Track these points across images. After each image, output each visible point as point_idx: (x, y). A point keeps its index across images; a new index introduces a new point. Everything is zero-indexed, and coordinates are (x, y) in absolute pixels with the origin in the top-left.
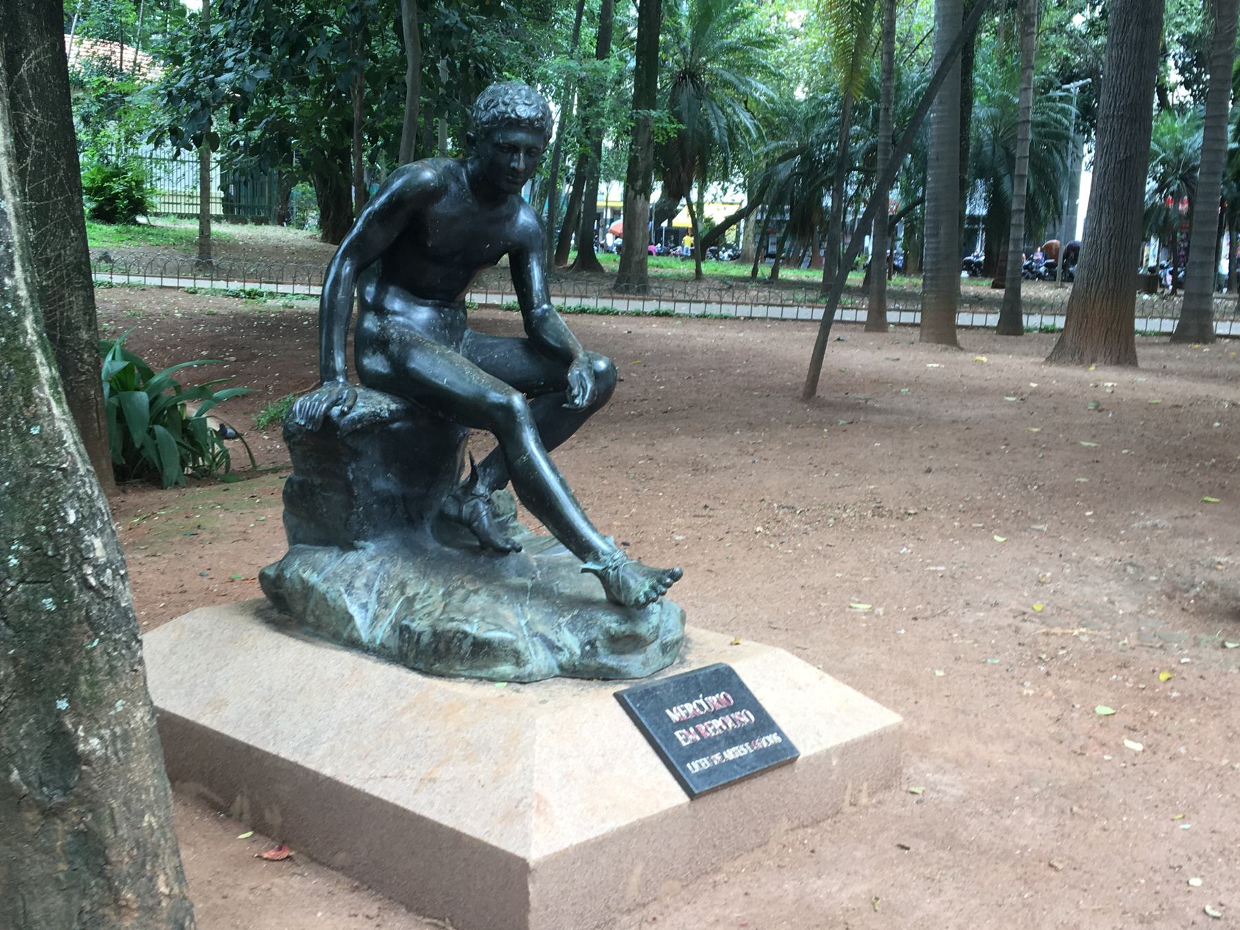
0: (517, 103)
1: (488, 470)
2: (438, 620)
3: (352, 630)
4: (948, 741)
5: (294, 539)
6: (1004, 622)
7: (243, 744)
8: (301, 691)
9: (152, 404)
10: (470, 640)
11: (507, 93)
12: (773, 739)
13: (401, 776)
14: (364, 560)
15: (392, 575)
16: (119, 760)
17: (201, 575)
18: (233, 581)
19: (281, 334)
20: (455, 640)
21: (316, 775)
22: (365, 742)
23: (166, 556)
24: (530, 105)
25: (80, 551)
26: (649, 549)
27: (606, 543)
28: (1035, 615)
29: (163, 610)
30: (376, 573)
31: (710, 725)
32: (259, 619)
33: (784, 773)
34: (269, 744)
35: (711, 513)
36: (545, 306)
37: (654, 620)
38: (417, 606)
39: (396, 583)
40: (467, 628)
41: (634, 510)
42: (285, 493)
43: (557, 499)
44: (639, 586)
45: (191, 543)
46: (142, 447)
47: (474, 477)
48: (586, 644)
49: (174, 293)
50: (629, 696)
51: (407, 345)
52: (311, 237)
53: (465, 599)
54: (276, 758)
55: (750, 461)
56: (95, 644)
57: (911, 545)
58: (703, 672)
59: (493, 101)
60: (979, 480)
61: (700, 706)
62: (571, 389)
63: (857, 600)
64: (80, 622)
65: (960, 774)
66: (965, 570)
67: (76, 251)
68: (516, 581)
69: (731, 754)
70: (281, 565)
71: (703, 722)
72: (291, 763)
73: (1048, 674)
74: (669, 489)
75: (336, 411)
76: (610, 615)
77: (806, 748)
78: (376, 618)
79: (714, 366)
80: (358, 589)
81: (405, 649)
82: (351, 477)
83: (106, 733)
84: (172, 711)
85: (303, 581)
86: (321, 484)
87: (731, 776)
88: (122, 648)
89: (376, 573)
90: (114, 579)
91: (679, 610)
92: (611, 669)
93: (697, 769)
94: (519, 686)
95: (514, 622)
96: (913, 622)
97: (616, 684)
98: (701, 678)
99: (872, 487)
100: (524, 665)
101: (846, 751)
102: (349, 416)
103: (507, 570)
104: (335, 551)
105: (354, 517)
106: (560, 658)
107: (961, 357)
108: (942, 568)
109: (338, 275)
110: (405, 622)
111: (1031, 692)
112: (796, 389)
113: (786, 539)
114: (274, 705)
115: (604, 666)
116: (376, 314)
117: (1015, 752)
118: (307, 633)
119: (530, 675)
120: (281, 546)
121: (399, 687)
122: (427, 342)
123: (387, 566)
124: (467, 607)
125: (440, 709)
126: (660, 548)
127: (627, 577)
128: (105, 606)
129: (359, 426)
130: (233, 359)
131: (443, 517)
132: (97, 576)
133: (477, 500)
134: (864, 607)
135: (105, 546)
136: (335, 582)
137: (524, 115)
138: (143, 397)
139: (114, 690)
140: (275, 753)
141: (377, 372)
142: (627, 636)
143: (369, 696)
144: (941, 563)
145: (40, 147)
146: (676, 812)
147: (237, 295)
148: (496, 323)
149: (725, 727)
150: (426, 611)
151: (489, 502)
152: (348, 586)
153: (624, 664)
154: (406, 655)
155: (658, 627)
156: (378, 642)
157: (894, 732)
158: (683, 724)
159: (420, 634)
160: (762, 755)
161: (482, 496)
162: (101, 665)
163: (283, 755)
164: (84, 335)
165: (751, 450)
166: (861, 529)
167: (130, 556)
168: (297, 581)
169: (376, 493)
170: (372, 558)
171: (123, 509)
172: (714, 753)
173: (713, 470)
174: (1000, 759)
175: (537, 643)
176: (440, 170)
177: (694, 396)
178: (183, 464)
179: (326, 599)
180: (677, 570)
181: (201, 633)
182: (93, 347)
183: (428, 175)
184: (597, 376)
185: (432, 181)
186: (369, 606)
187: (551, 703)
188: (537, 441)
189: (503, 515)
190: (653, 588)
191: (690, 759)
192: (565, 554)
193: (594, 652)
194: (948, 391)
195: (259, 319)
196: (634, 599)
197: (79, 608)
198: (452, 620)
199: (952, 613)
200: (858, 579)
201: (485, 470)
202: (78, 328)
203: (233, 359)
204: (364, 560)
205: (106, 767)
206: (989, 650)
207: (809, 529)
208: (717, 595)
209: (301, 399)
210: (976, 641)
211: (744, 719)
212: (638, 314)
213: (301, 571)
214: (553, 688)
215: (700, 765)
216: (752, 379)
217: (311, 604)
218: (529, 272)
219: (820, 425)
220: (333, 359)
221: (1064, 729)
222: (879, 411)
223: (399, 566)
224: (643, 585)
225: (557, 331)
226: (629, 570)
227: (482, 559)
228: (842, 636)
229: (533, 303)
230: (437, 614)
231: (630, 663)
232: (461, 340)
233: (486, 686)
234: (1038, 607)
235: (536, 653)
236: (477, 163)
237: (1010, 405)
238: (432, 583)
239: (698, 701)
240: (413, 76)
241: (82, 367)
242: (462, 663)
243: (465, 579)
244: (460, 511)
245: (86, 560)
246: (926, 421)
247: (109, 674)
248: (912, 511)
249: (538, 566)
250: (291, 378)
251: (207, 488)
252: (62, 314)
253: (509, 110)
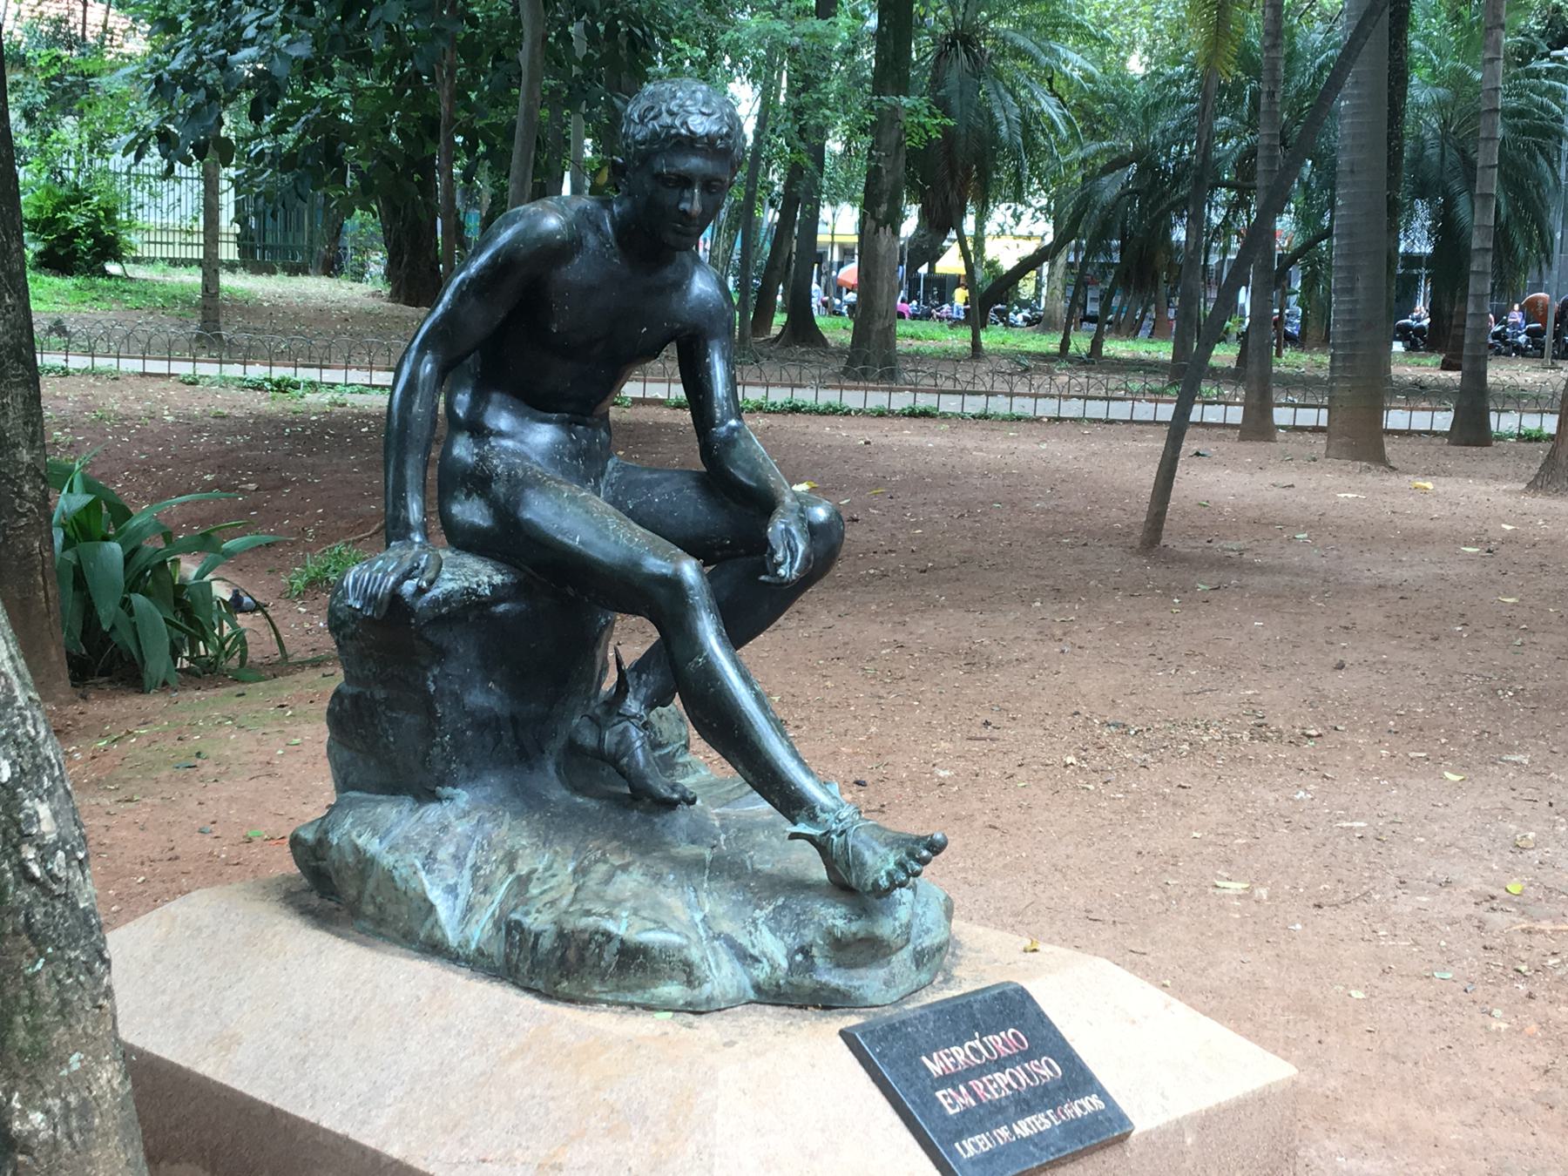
0: (691, 113)
1: (644, 677)
2: (566, 912)
3: (433, 927)
4: (1371, 1106)
5: (344, 784)
6: (1461, 912)
7: (264, 1105)
8: (354, 1023)
9: (128, 559)
10: (615, 945)
11: (674, 97)
12: (1092, 1103)
13: (509, 1159)
14: (452, 818)
15: (495, 840)
16: (74, 1146)
17: (201, 831)
18: (250, 841)
19: (328, 448)
20: (593, 946)
21: (376, 1156)
22: (453, 1105)
23: (144, 800)
24: (709, 115)
25: (17, 823)
26: (898, 790)
27: (828, 793)
28: (1508, 901)
29: (141, 888)
30: (471, 838)
31: (991, 1082)
32: (291, 909)
33: (1110, 1157)
34: (304, 1106)
35: (996, 734)
36: (733, 423)
37: (903, 914)
38: (534, 890)
39: (501, 853)
40: (610, 926)
41: (873, 729)
42: (330, 712)
43: (752, 726)
44: (880, 862)
45: (185, 781)
46: (113, 628)
47: (622, 688)
48: (797, 952)
49: (162, 384)
50: (864, 1036)
51: (519, 484)
52: (373, 295)
53: (608, 879)
54: (315, 1128)
55: (1057, 650)
56: (39, 966)
57: (1312, 787)
58: (980, 997)
59: (652, 108)
60: (1422, 681)
61: (975, 1051)
62: (773, 553)
63: (1226, 875)
64: (16, 933)
65: (1390, 1158)
66: (1398, 828)
67: (13, 326)
68: (686, 850)
69: (1024, 1128)
70: (324, 826)
71: (979, 1078)
72: (337, 1136)
73: (1530, 996)
74: (928, 695)
75: (409, 587)
76: (834, 906)
77: (1144, 1116)
78: (470, 908)
79: (1000, 497)
80: (443, 862)
81: (514, 958)
82: (432, 688)
83: (55, 1104)
84: (156, 1052)
85: (357, 850)
86: (386, 699)
87: (1025, 1163)
88: (80, 973)
89: (471, 838)
90: (68, 865)
91: (942, 898)
92: (837, 991)
93: (972, 1152)
94: (691, 1017)
95: (683, 914)
96: (1315, 911)
97: (843, 1015)
98: (976, 1006)
99: (1250, 692)
100: (700, 985)
101: (1206, 1122)
102: (429, 595)
103: (673, 834)
104: (408, 802)
105: (437, 750)
106: (755, 973)
107: (1392, 481)
108: (1363, 824)
109: (413, 375)
110: (515, 916)
111: (1504, 1026)
112: (1129, 534)
113: (1113, 777)
114: (312, 1044)
115: (824, 986)
116: (472, 436)
117: (1478, 1124)
118: (363, 931)
119: (709, 1000)
120: (324, 790)
121: (506, 1018)
122: (549, 479)
123: (488, 826)
124: (611, 892)
125: (569, 1055)
126: (915, 791)
127: (861, 847)
128: (54, 907)
129: (444, 610)
130: (252, 486)
131: (573, 749)
132: (43, 862)
133: (627, 723)
134: (1237, 887)
135: (55, 815)
136: (407, 851)
137: (700, 130)
138: (115, 549)
139: (67, 1037)
140: (313, 1120)
141: (472, 525)
142: (861, 940)
143: (459, 1033)
144: (1360, 816)
147: (258, 387)
148: (658, 427)
149: (1015, 1085)
150: (547, 898)
151: (646, 726)
152: (427, 858)
153: (856, 983)
154: (517, 966)
155: (909, 926)
156: (473, 946)
157: (1283, 1092)
158: (948, 1080)
159: (538, 935)
160: (1075, 1129)
161: (634, 716)
162: (48, 1000)
163: (325, 1124)
164: (25, 456)
165: (1058, 632)
166: (1233, 760)
167: (93, 802)
168: (348, 849)
169: (471, 714)
170: (466, 814)
171: (82, 725)
172: (998, 1126)
173: (999, 665)
174: (1453, 1136)
175: (720, 950)
176: (571, 214)
177: (968, 544)
178: (175, 653)
179: (393, 879)
180: (938, 836)
181: (199, 930)
182: (38, 474)
183: (552, 222)
184: (813, 530)
185: (558, 232)
186: (459, 890)
187: (741, 1043)
188: (719, 634)
189: (668, 744)
190: (901, 865)
191: (959, 1135)
192: (762, 808)
193: (809, 966)
194: (1369, 537)
195: (292, 423)
196: (870, 881)
197: (15, 912)
198: (588, 913)
199: (1377, 897)
200: (1227, 841)
201: (639, 677)
202: (16, 445)
203: (252, 486)
204: (452, 818)
205: (54, 1156)
206: (1437, 956)
207: (1150, 760)
208: (1005, 866)
209: (357, 568)
210: (1416, 943)
211: (1046, 1072)
212: (881, 414)
213: (354, 834)
214: (745, 1021)
215: (976, 1146)
216: (1059, 518)
217: (371, 884)
218: (708, 369)
219: (1168, 592)
220: (406, 507)
221: (1555, 1086)
222: (1262, 569)
223: (505, 827)
224: (885, 860)
225: (751, 460)
226: (863, 835)
227: (635, 815)
228: (1202, 934)
229: (712, 418)
230: (565, 902)
231: (866, 982)
232: (603, 474)
233: (640, 1018)
234: (1515, 888)
235: (718, 966)
236: (627, 203)
237: (1470, 559)
238: (556, 853)
239: (972, 1044)
240: (532, 55)
241: (20, 506)
242: (602, 980)
243: (608, 847)
244: (601, 740)
245: (25, 837)
246: (1338, 588)
247: (60, 1012)
248: (1313, 733)
249: (722, 826)
250: (342, 517)
251: (211, 692)
253: (677, 123)
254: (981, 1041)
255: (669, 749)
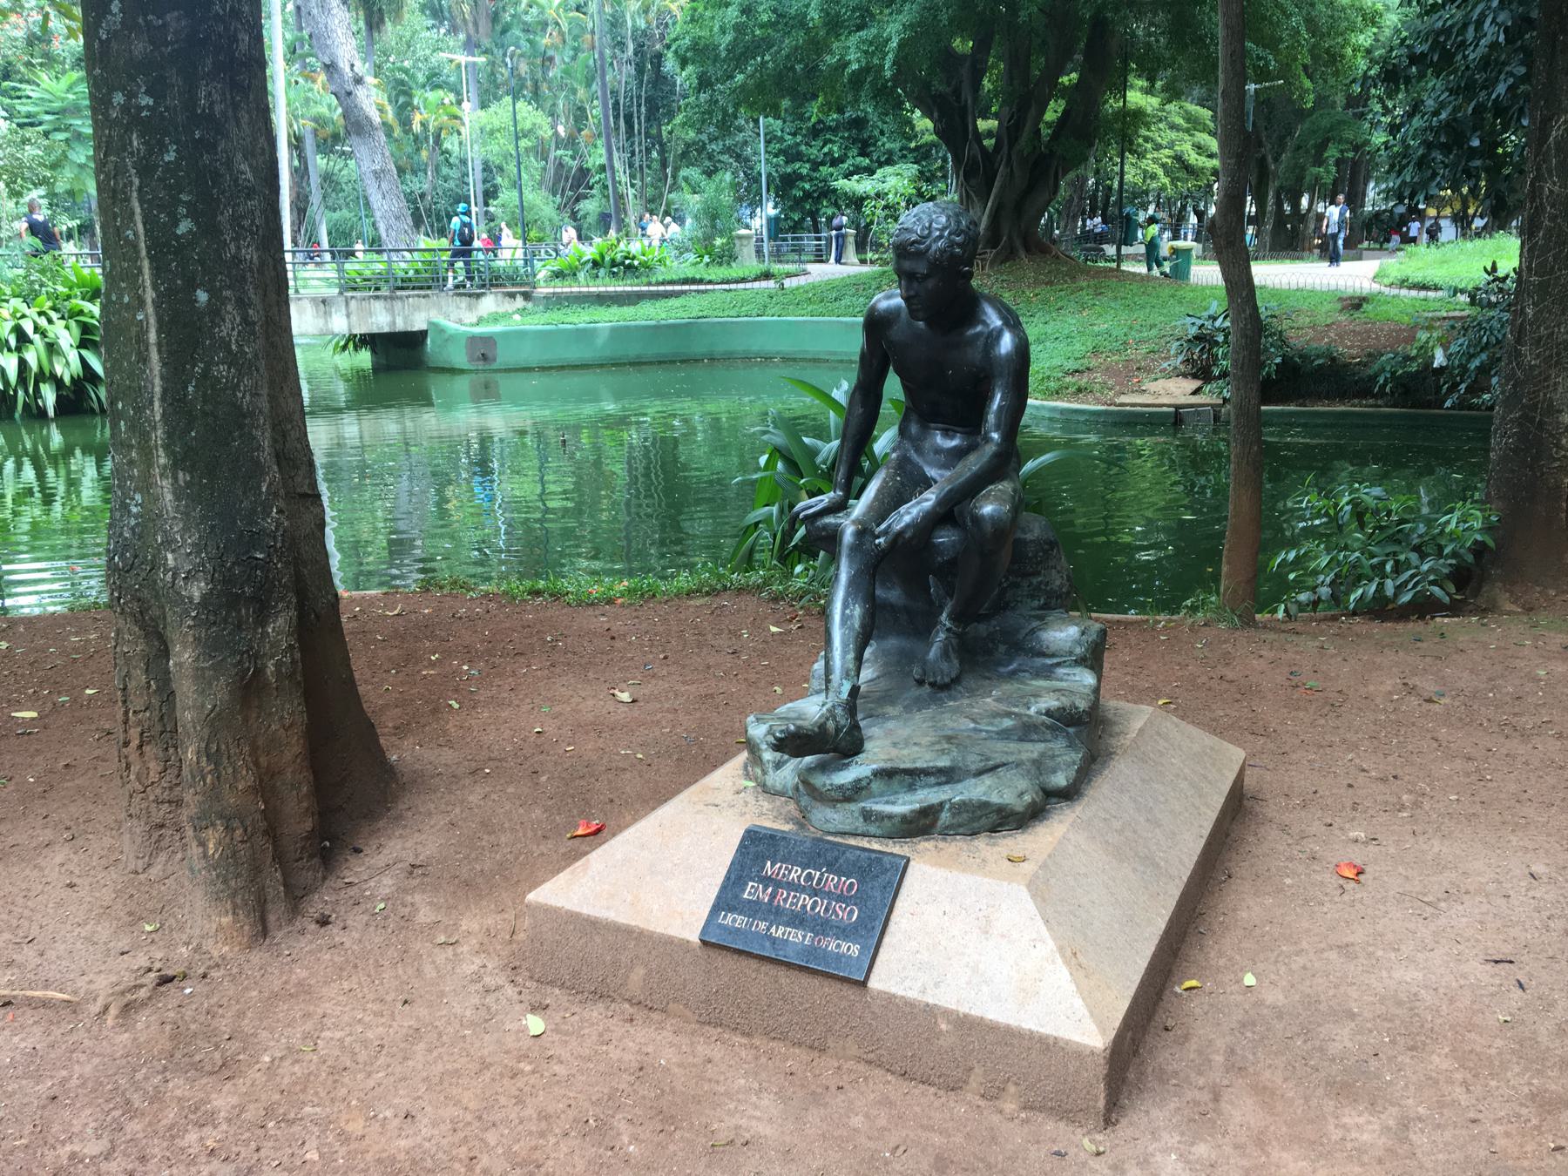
33: (850, 993)
61: (809, 877)
69: (778, 932)
101: (967, 1025)
145: (1553, 218)
146: (684, 945)
189: (1053, 655)
215: (734, 920)
252: (1545, 395)
254: (822, 874)
255: (1049, 661)
